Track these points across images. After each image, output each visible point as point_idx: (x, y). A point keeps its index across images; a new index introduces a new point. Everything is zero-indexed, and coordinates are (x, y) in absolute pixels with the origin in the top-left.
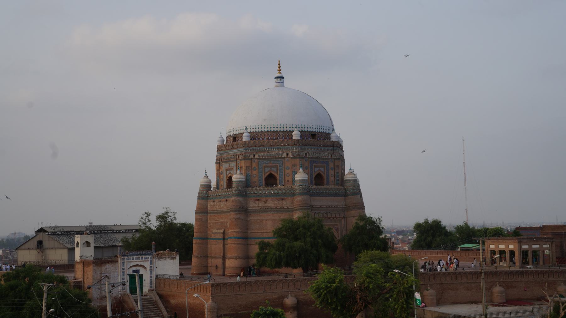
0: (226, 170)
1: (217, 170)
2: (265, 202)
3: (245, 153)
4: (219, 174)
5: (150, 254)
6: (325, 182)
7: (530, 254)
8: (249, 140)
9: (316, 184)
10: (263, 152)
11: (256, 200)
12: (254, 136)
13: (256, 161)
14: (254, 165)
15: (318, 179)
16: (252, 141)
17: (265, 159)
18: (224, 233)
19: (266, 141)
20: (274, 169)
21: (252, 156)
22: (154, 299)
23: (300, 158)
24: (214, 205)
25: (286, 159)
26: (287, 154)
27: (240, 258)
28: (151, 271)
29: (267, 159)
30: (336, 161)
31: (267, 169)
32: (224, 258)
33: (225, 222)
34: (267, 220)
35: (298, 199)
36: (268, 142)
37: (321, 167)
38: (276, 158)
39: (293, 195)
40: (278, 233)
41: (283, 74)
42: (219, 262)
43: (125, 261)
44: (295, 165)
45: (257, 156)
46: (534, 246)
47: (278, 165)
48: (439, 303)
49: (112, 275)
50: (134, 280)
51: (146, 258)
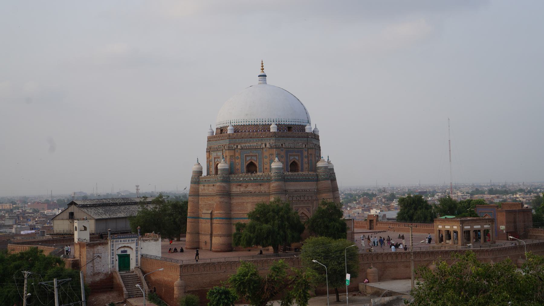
0: (215, 158)
1: (207, 158)
2: (246, 187)
3: (229, 144)
4: (209, 162)
5: (136, 237)
6: (300, 169)
7: (472, 234)
8: (233, 132)
9: (291, 171)
10: (245, 143)
11: (238, 185)
12: (237, 129)
13: (239, 151)
14: (237, 155)
15: (294, 167)
16: (235, 134)
17: (246, 149)
18: (211, 213)
19: (248, 133)
20: (255, 158)
21: (235, 147)
22: (138, 275)
23: (276, 148)
24: (204, 189)
25: (264, 150)
26: (266, 145)
27: (224, 236)
28: (137, 251)
29: (248, 149)
30: (309, 150)
31: (248, 158)
32: (211, 235)
33: (209, 206)
34: (247, 203)
35: (274, 184)
36: (249, 134)
37: (296, 155)
38: (256, 149)
39: (269, 181)
40: (251, 216)
41: (266, 72)
42: (207, 238)
43: (114, 243)
44: (272, 154)
45: (239, 147)
46: (476, 227)
47: (257, 154)
48: (381, 279)
49: (103, 255)
50: (124, 260)
51: (133, 240)
